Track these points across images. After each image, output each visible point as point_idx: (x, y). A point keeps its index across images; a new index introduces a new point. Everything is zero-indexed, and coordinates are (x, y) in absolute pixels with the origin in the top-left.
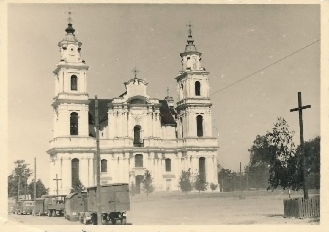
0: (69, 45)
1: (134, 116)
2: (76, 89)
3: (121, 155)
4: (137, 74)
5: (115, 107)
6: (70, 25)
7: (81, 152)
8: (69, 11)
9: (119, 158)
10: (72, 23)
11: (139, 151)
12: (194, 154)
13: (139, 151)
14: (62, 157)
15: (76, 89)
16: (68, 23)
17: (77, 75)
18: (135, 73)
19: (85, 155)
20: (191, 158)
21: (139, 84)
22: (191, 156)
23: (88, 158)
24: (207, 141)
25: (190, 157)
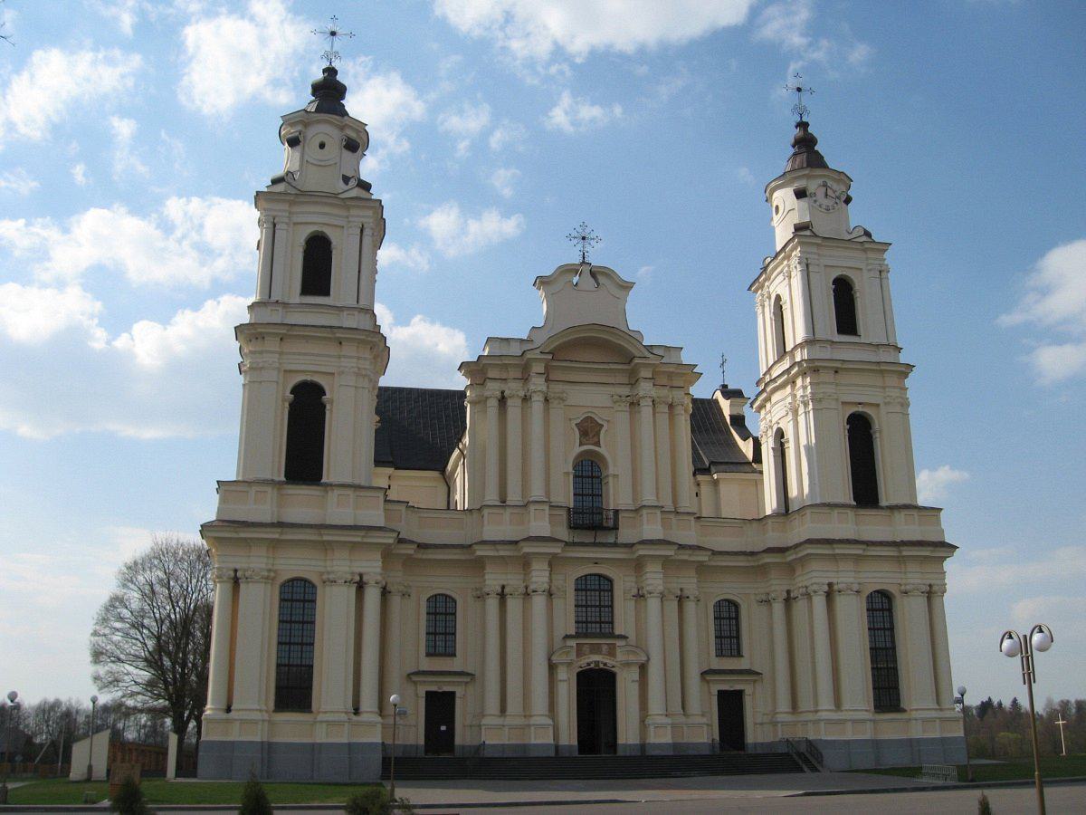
0: (311, 132)
1: (579, 416)
2: (326, 292)
3: (513, 580)
4: (588, 248)
5: (491, 374)
6: (331, 72)
7: (326, 547)
8: (331, 27)
9: (507, 590)
10: (336, 64)
11: (596, 562)
12: (844, 576)
13: (596, 562)
14: (236, 571)
15: (326, 292)
16: (325, 65)
17: (329, 232)
18: (580, 246)
19: (342, 565)
20: (830, 596)
21: (598, 284)
22: (830, 585)
23: (357, 578)
24: (900, 517)
25: (826, 588)
